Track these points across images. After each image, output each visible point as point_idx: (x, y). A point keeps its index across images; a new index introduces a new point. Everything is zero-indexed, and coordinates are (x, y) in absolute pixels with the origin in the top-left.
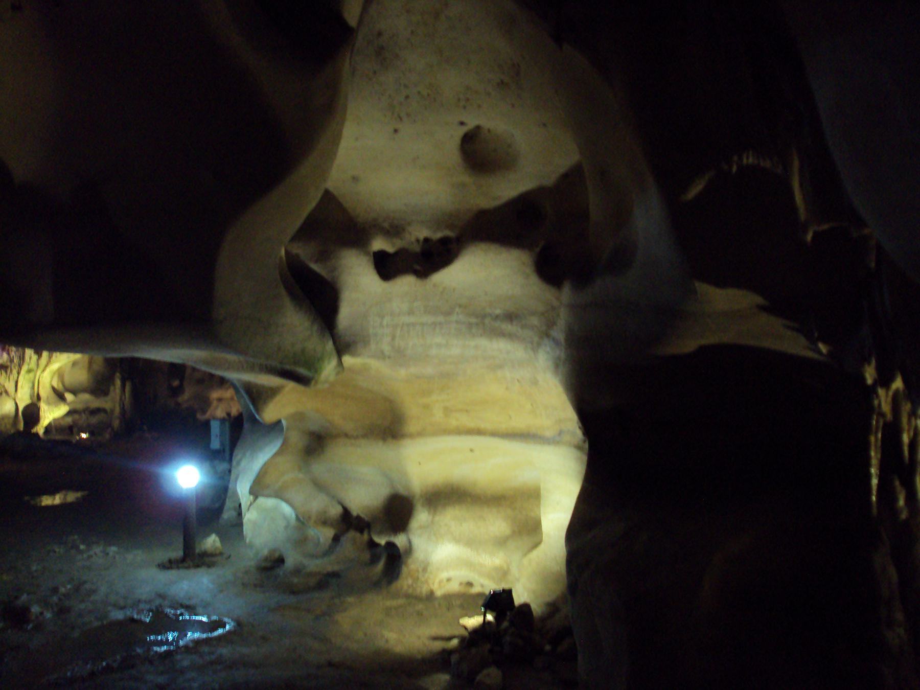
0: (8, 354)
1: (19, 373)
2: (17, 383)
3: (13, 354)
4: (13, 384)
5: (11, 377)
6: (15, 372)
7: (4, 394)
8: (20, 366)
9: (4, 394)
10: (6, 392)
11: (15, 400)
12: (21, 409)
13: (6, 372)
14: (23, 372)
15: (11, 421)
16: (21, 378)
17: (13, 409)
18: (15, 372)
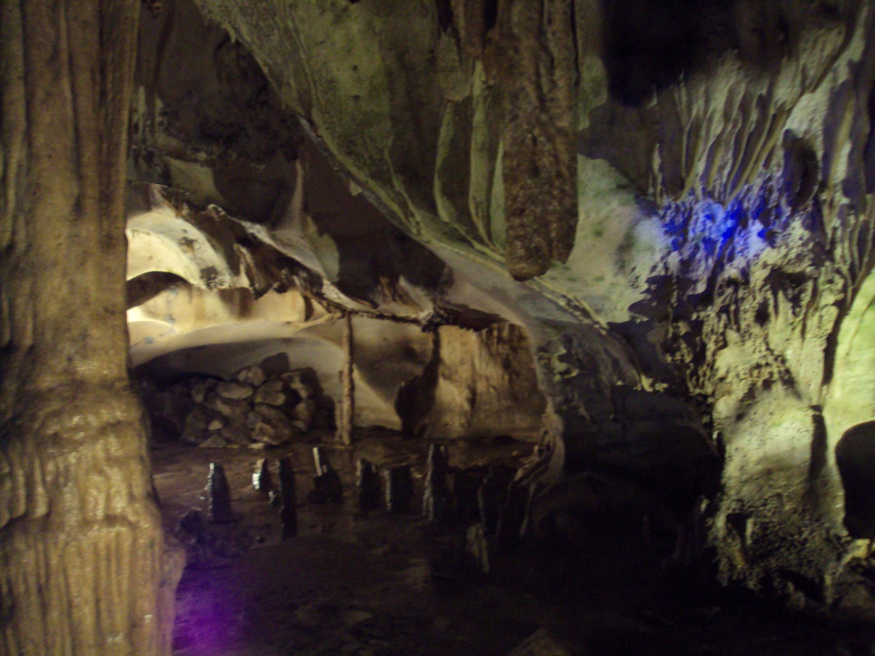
0: (815, 223)
1: (843, 307)
2: (832, 341)
3: (832, 222)
4: (815, 348)
5: (813, 322)
6: (828, 299)
7: (778, 388)
8: (854, 279)
9: (778, 388)
10: (789, 381)
11: (818, 408)
12: (834, 438)
13: (795, 301)
14: (859, 303)
15: (797, 485)
16: (848, 324)
17: (805, 440)
18: (828, 299)
